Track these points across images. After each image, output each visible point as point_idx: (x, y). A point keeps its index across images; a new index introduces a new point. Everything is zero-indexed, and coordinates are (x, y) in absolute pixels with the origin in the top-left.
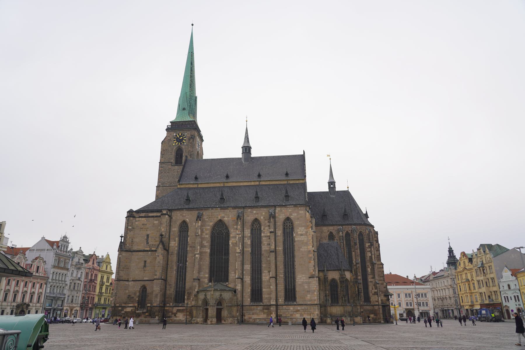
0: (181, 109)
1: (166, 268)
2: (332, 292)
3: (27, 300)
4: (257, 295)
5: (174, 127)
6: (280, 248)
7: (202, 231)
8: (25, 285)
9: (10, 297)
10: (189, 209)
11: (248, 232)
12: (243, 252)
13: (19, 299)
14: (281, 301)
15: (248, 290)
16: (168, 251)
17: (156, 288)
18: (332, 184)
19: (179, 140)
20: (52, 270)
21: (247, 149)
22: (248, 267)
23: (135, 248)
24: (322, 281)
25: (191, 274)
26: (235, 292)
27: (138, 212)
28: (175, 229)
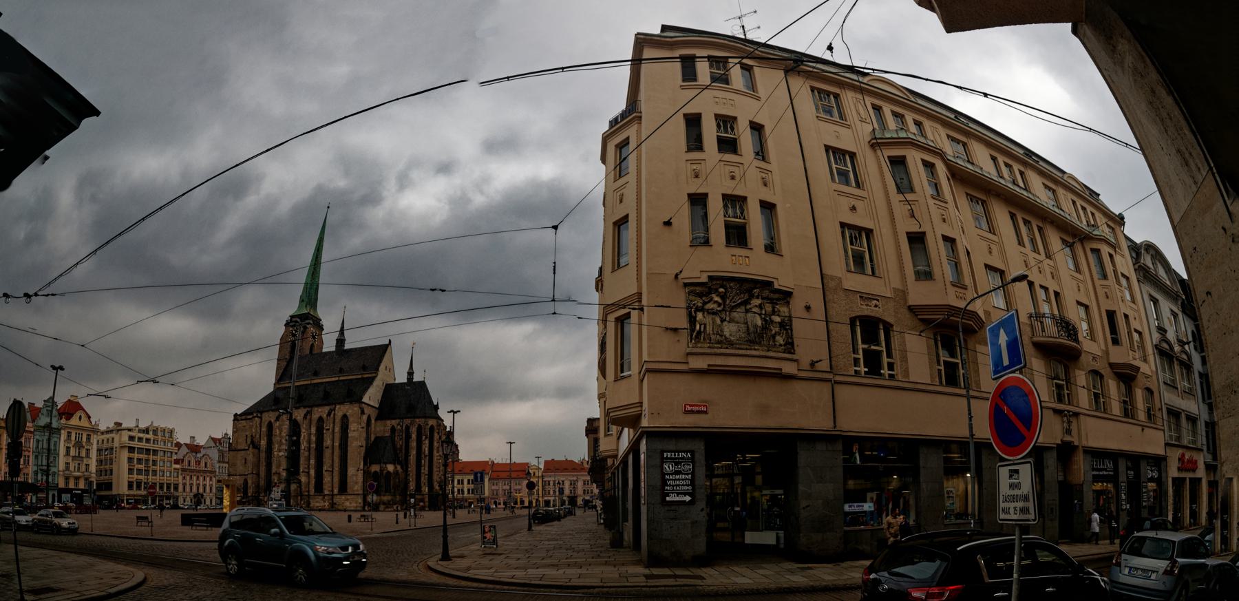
2: (376, 483)
4: (319, 487)
7: (281, 431)
14: (336, 491)
15: (313, 482)
22: (312, 462)
24: (366, 473)
26: (300, 482)
28: (264, 429)
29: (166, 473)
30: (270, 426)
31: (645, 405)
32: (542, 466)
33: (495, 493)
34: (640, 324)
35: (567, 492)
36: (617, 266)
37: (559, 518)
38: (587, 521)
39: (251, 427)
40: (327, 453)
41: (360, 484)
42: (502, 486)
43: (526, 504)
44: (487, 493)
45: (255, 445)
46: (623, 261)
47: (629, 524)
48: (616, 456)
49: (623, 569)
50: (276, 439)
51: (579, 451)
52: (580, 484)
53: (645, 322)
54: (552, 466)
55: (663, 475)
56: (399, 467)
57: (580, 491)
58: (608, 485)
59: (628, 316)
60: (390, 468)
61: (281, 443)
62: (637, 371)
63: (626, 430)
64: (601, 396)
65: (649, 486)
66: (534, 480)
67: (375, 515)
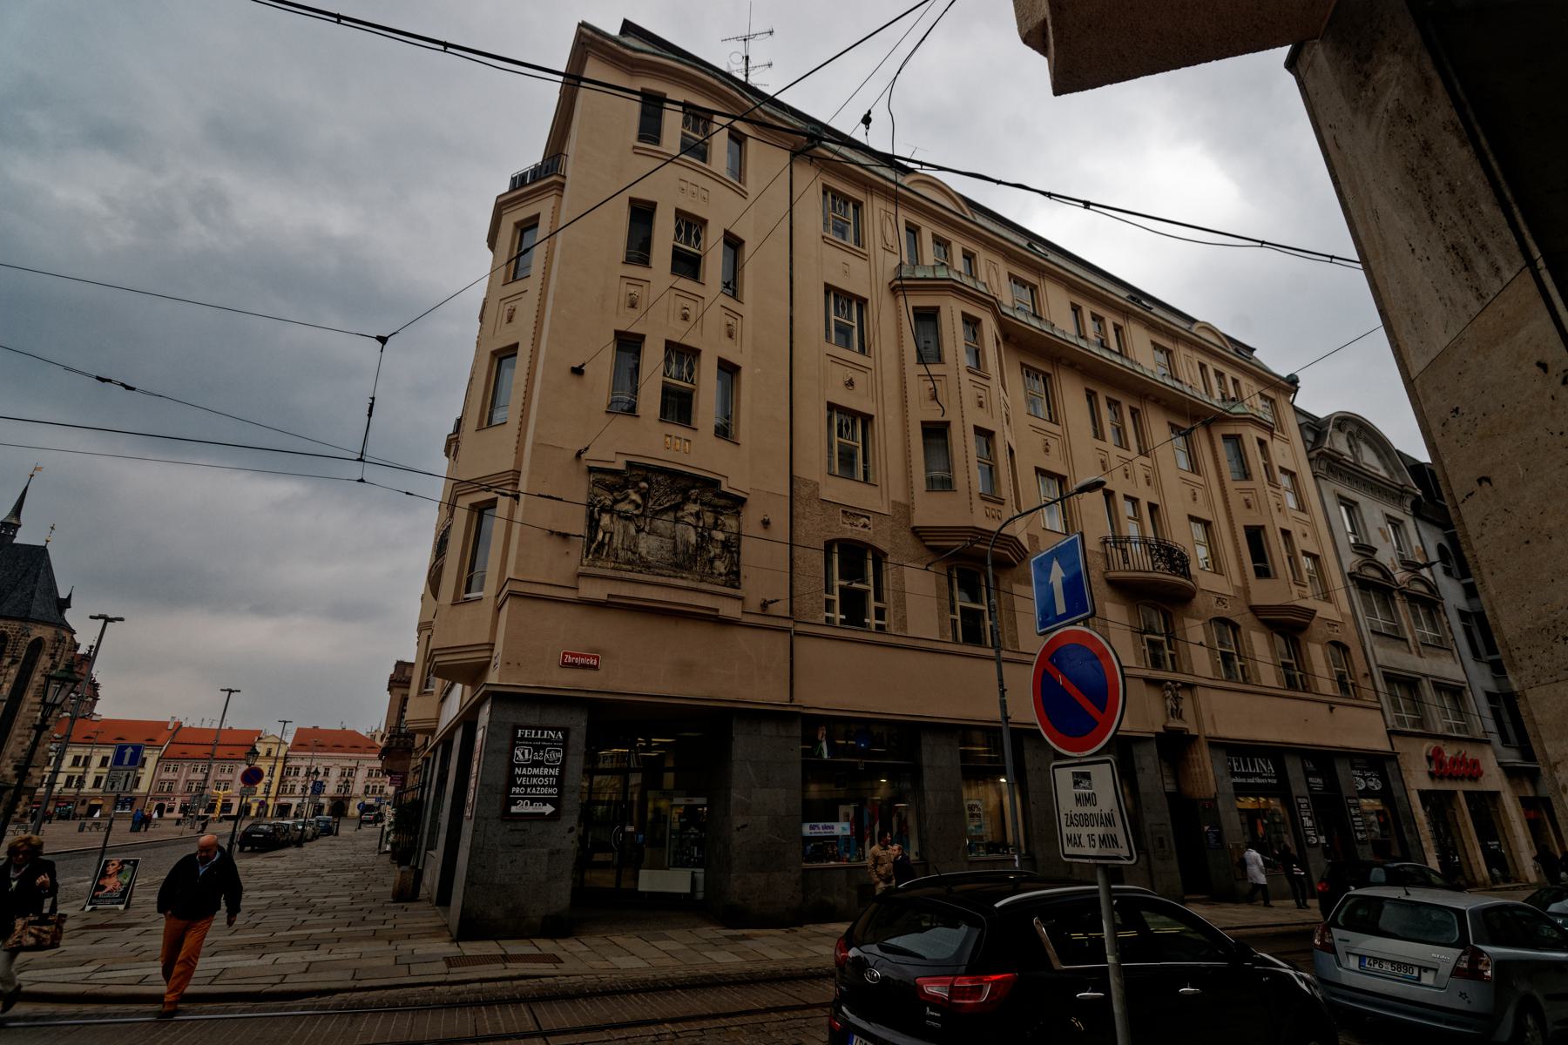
31: (499, 648)
32: (289, 739)
33: (163, 791)
34: (510, 520)
35: (331, 789)
36: (487, 421)
37: (300, 842)
38: (359, 844)
42: (186, 774)
43: (234, 812)
44: (143, 787)
46: (498, 416)
47: (438, 854)
48: (432, 731)
51: (371, 716)
52: (361, 776)
53: (518, 516)
54: (309, 741)
55: (512, 766)
57: (358, 788)
58: (412, 780)
59: (492, 504)
62: (494, 593)
63: (459, 687)
64: (424, 627)
65: (483, 786)
66: (265, 766)
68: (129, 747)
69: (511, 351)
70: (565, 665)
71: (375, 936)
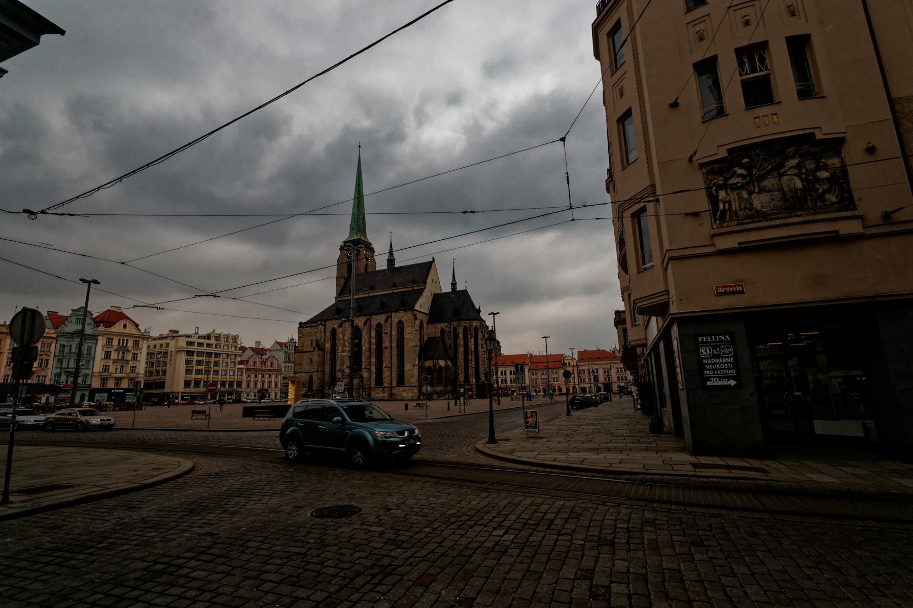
0: (352, 229)
1: (323, 364)
2: (429, 376)
3: (266, 386)
4: (379, 381)
5: (345, 247)
6: (394, 345)
7: (344, 335)
8: (263, 376)
9: (252, 385)
10: (336, 319)
11: (373, 334)
12: (370, 350)
13: (259, 386)
14: (394, 384)
15: (374, 376)
16: (324, 351)
17: (315, 378)
18: (454, 284)
19: (349, 257)
20: (283, 365)
21: (391, 261)
22: (373, 360)
23: (305, 350)
24: (421, 368)
25: (338, 367)
26: (362, 377)
27: (305, 323)
28: (328, 334)
29: (227, 372)
30: (334, 332)
31: (672, 292)
32: (576, 357)
33: (534, 382)
34: (657, 216)
35: (601, 379)
36: (626, 163)
37: (595, 404)
38: (624, 407)
39: (316, 333)
40: (386, 353)
41: (416, 377)
42: (540, 376)
43: (564, 391)
44: (527, 383)
45: (320, 347)
46: (632, 156)
47: (668, 410)
48: (645, 345)
49: (666, 456)
50: (338, 342)
51: (610, 341)
52: (613, 372)
53: (662, 211)
54: (585, 356)
55: (700, 359)
56: (449, 363)
58: (642, 372)
59: (644, 209)
60: (442, 363)
61: (344, 346)
62: (660, 261)
63: (654, 319)
64: (623, 290)
65: (686, 372)
66: (570, 369)
67: (429, 403)
68: (520, 363)
69: (628, 113)
70: (719, 294)
71: (647, 449)
